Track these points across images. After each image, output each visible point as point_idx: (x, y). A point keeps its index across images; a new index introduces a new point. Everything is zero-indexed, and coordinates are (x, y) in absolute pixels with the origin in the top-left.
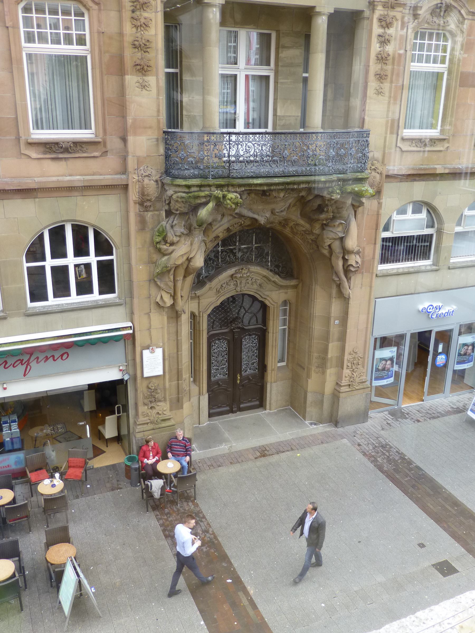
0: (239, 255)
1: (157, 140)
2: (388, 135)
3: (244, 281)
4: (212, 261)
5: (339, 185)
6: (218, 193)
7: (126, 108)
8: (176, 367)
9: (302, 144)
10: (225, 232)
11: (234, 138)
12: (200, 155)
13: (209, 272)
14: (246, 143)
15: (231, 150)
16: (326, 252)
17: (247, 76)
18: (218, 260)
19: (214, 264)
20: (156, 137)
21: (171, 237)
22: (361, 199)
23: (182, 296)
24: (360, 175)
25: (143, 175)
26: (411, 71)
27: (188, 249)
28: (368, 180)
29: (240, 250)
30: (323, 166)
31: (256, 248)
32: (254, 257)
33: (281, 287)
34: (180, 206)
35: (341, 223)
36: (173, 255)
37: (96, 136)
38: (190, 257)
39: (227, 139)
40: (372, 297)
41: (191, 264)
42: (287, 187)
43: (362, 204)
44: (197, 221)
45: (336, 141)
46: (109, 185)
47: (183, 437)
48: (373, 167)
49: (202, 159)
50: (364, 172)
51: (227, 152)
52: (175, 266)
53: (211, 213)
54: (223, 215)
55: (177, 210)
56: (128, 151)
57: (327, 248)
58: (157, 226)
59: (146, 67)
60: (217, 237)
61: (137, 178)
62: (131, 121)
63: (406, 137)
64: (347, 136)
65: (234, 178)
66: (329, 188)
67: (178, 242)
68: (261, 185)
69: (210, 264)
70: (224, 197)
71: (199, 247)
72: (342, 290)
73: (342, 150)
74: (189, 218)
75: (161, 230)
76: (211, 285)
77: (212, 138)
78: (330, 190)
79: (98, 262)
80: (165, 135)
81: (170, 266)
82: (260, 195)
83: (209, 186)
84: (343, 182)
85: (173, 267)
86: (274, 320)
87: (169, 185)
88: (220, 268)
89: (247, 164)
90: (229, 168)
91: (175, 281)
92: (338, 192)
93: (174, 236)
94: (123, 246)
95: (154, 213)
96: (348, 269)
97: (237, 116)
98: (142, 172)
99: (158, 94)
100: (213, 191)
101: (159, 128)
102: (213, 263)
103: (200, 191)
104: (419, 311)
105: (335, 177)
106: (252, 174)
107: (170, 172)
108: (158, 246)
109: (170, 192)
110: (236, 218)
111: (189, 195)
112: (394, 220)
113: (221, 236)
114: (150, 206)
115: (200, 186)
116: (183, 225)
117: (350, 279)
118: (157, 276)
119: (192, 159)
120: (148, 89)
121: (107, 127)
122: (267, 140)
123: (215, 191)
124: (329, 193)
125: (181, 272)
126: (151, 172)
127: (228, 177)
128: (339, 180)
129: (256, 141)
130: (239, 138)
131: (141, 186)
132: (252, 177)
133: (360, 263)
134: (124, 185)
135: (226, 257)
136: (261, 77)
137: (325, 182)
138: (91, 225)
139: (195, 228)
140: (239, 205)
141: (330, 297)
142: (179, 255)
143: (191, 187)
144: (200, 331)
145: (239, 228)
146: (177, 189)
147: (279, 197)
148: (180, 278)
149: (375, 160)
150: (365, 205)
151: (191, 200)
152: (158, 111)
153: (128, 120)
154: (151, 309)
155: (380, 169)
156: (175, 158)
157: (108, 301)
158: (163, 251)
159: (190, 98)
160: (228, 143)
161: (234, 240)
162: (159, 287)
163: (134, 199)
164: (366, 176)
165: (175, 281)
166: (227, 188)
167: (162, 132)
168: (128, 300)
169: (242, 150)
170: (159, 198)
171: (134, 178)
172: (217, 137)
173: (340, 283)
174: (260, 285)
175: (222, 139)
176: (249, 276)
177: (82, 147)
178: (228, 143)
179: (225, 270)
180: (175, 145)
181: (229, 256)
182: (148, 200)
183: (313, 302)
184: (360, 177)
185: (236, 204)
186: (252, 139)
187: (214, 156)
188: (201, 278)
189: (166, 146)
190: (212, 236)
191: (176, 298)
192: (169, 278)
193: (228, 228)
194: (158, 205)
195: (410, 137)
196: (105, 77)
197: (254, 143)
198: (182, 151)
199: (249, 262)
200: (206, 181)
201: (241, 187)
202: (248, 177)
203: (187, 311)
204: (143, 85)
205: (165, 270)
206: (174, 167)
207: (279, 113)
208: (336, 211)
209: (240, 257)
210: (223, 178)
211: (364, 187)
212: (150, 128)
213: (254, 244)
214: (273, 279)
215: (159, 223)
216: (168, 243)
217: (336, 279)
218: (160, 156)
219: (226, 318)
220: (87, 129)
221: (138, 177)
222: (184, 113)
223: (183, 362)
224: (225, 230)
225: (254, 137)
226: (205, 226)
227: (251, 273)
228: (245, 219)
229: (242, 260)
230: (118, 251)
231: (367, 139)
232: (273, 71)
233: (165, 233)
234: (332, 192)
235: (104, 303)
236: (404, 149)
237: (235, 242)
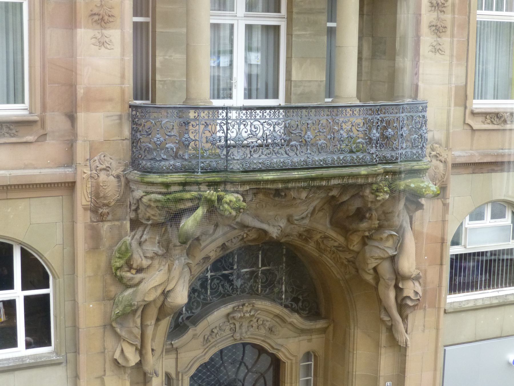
0: (238, 283)
1: (120, 117)
2: (452, 108)
3: (245, 324)
4: (196, 294)
5: (386, 180)
6: (210, 193)
7: (76, 73)
9: (331, 123)
10: (219, 250)
11: (233, 114)
12: (184, 139)
13: (193, 311)
14: (252, 121)
15: (229, 131)
16: (369, 278)
17: (249, 28)
18: (207, 293)
19: (200, 299)
20: (119, 113)
21: (138, 260)
22: (420, 200)
23: (153, 350)
24: (416, 165)
25: (98, 168)
26: (477, 21)
27: (165, 278)
28: (428, 171)
29: (238, 277)
30: (362, 153)
31: (263, 272)
32: (260, 286)
33: (302, 331)
34: (153, 213)
35: (392, 235)
36: (141, 287)
37: (31, 113)
38: (167, 289)
39: (223, 116)
40: (440, 344)
41: (169, 300)
42: (312, 184)
43: (420, 206)
44: (179, 236)
45: (380, 117)
46: (47, 184)
48: (434, 153)
49: (186, 145)
50: (420, 160)
51: (223, 135)
52: (144, 303)
53: (200, 224)
54: (217, 226)
55: (148, 219)
56: (77, 134)
57: (372, 271)
58: (118, 243)
59: (106, 18)
60: (207, 258)
61: (89, 172)
62: (82, 91)
63: (476, 111)
64: (396, 111)
65: (233, 172)
66: (372, 184)
67: (149, 267)
68: (273, 181)
69: (194, 298)
70: (220, 199)
71: (181, 274)
72: (396, 336)
73: (390, 130)
74: (166, 230)
75: (123, 248)
76: (195, 330)
77: (202, 115)
78: (375, 187)
79: (27, 299)
80: (132, 111)
81: (136, 303)
82: (271, 196)
83: (198, 184)
84: (392, 175)
85: (141, 305)
87: (136, 182)
88: (210, 303)
89: (252, 152)
90: (227, 157)
91: (143, 327)
92: (385, 190)
93: (143, 258)
94: (65, 274)
95: (113, 223)
96: (404, 302)
97: (234, 81)
98: (97, 163)
99: (123, 54)
100: (203, 191)
101: (123, 100)
102: (199, 296)
103: (184, 191)
104: (509, 363)
105: (380, 168)
106: (260, 166)
107: (138, 164)
108: (118, 273)
109: (138, 193)
110: (235, 229)
111: (168, 197)
112: (466, 229)
113: (214, 256)
114: (108, 213)
115: (184, 184)
116: (157, 241)
117: (407, 317)
118: (116, 320)
119: (172, 146)
120: (108, 47)
121: (48, 100)
122: (281, 117)
123: (206, 191)
124: (373, 191)
125: (153, 312)
126: (111, 164)
127: (225, 170)
128: (386, 173)
129: (265, 119)
130: (241, 115)
131: (94, 184)
132: (261, 171)
133: (421, 293)
134: (68, 183)
135: (219, 286)
136: (266, 28)
137: (367, 176)
138: (16, 242)
139: (175, 246)
140: (242, 210)
141: (378, 345)
142: (151, 286)
143: (171, 186)
145: (239, 243)
146: (150, 189)
147: (300, 199)
148: (151, 322)
149: (436, 143)
150: (425, 207)
151: (171, 205)
152: (123, 77)
153: (78, 89)
154: (106, 370)
155: (445, 155)
156: (145, 142)
157: (40, 358)
158: (125, 281)
159: (167, 57)
160: (225, 122)
161: (231, 260)
162: (118, 337)
163: (84, 202)
164: (425, 167)
165: (143, 327)
166: (223, 186)
167: (127, 106)
168: (70, 356)
169: (246, 132)
170: (120, 202)
171: (85, 173)
172: (209, 113)
173: (392, 325)
174: (271, 330)
175: (216, 116)
176: (253, 315)
177: (11, 129)
178: (225, 122)
179: (217, 306)
180: (148, 125)
181: (223, 286)
182: (105, 205)
183: (351, 355)
184: (417, 167)
185: (238, 210)
186: (260, 116)
187: (204, 140)
188: (180, 320)
189: (133, 126)
190: (200, 256)
191: (144, 352)
192: (134, 322)
193: (224, 244)
194: (120, 212)
195: (483, 111)
196: (48, 32)
197: (262, 121)
198: (158, 134)
199: (253, 293)
200: (193, 177)
201: (244, 185)
202: (254, 171)
204: (102, 41)
205: (128, 309)
206: (145, 156)
207: (294, 78)
208: (383, 217)
209: (239, 287)
210: (218, 172)
211: (423, 182)
212: (111, 100)
213: (260, 266)
214: (289, 320)
215: (120, 239)
216: (134, 269)
217: (386, 318)
218: (123, 140)
220: (17, 103)
221: (91, 171)
222: (158, 77)
224: (218, 247)
225: (263, 113)
226: (189, 243)
228: (249, 231)
229: (243, 291)
230: (58, 280)
231: (423, 114)
232: (285, 20)
233: (130, 254)
234: (377, 190)
235: (33, 361)
236: (475, 127)
237: (232, 264)
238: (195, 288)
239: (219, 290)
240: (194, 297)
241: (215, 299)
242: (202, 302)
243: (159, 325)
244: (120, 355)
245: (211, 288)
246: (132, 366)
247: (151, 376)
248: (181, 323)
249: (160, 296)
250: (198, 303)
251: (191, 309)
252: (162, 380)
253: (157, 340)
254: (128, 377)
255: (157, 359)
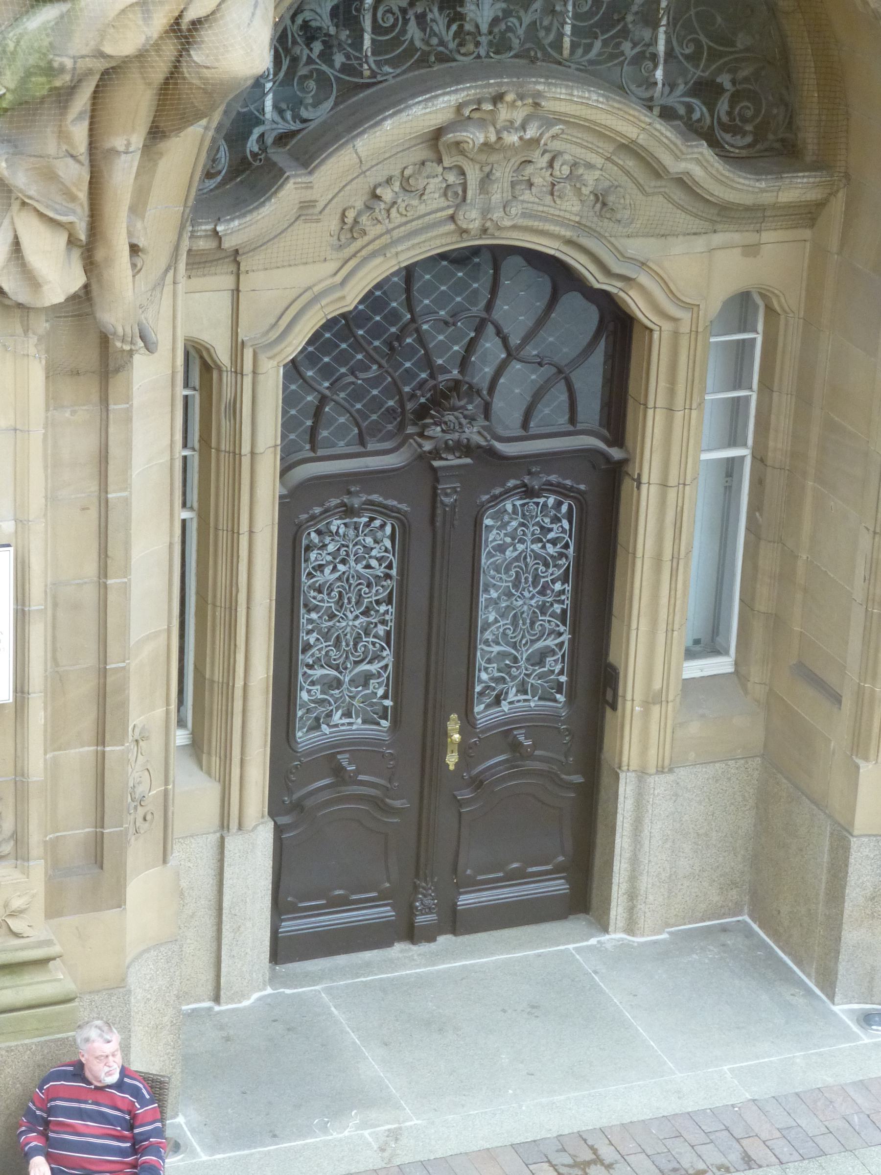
3: (503, 174)
4: (317, 47)
8: (90, 660)
13: (304, 114)
18: (358, 43)
19: (332, 66)
23: (134, 249)
32: (568, 29)
38: (192, 14)
41: (197, 56)
47: (124, 1072)
52: (100, 65)
69: (310, 60)
76: (309, 186)
81: (69, 63)
85: (89, 72)
86: (670, 409)
88: (369, 86)
102: (326, 56)
135: (406, 21)
144: (236, 455)
174: (601, 200)
176: (535, 142)
181: (421, 19)
188: (252, 144)
191: (100, 255)
192: (63, 135)
203: (163, 336)
205: (39, 86)
209: (484, 28)
214: (676, 167)
219: (395, 389)
223: (136, 634)
227: (549, 122)
229: (501, 46)
238: (313, 24)
239: (408, 36)
240: (309, 57)
241: (387, 69)
242: (337, 78)
243: (161, 154)
244: (9, 260)
245: (377, 28)
246: (55, 308)
247: (127, 347)
248: (255, 155)
249: (161, 38)
250: (323, 81)
251: (296, 104)
252: (174, 366)
253: (151, 212)
254: (36, 346)
255: (154, 289)
